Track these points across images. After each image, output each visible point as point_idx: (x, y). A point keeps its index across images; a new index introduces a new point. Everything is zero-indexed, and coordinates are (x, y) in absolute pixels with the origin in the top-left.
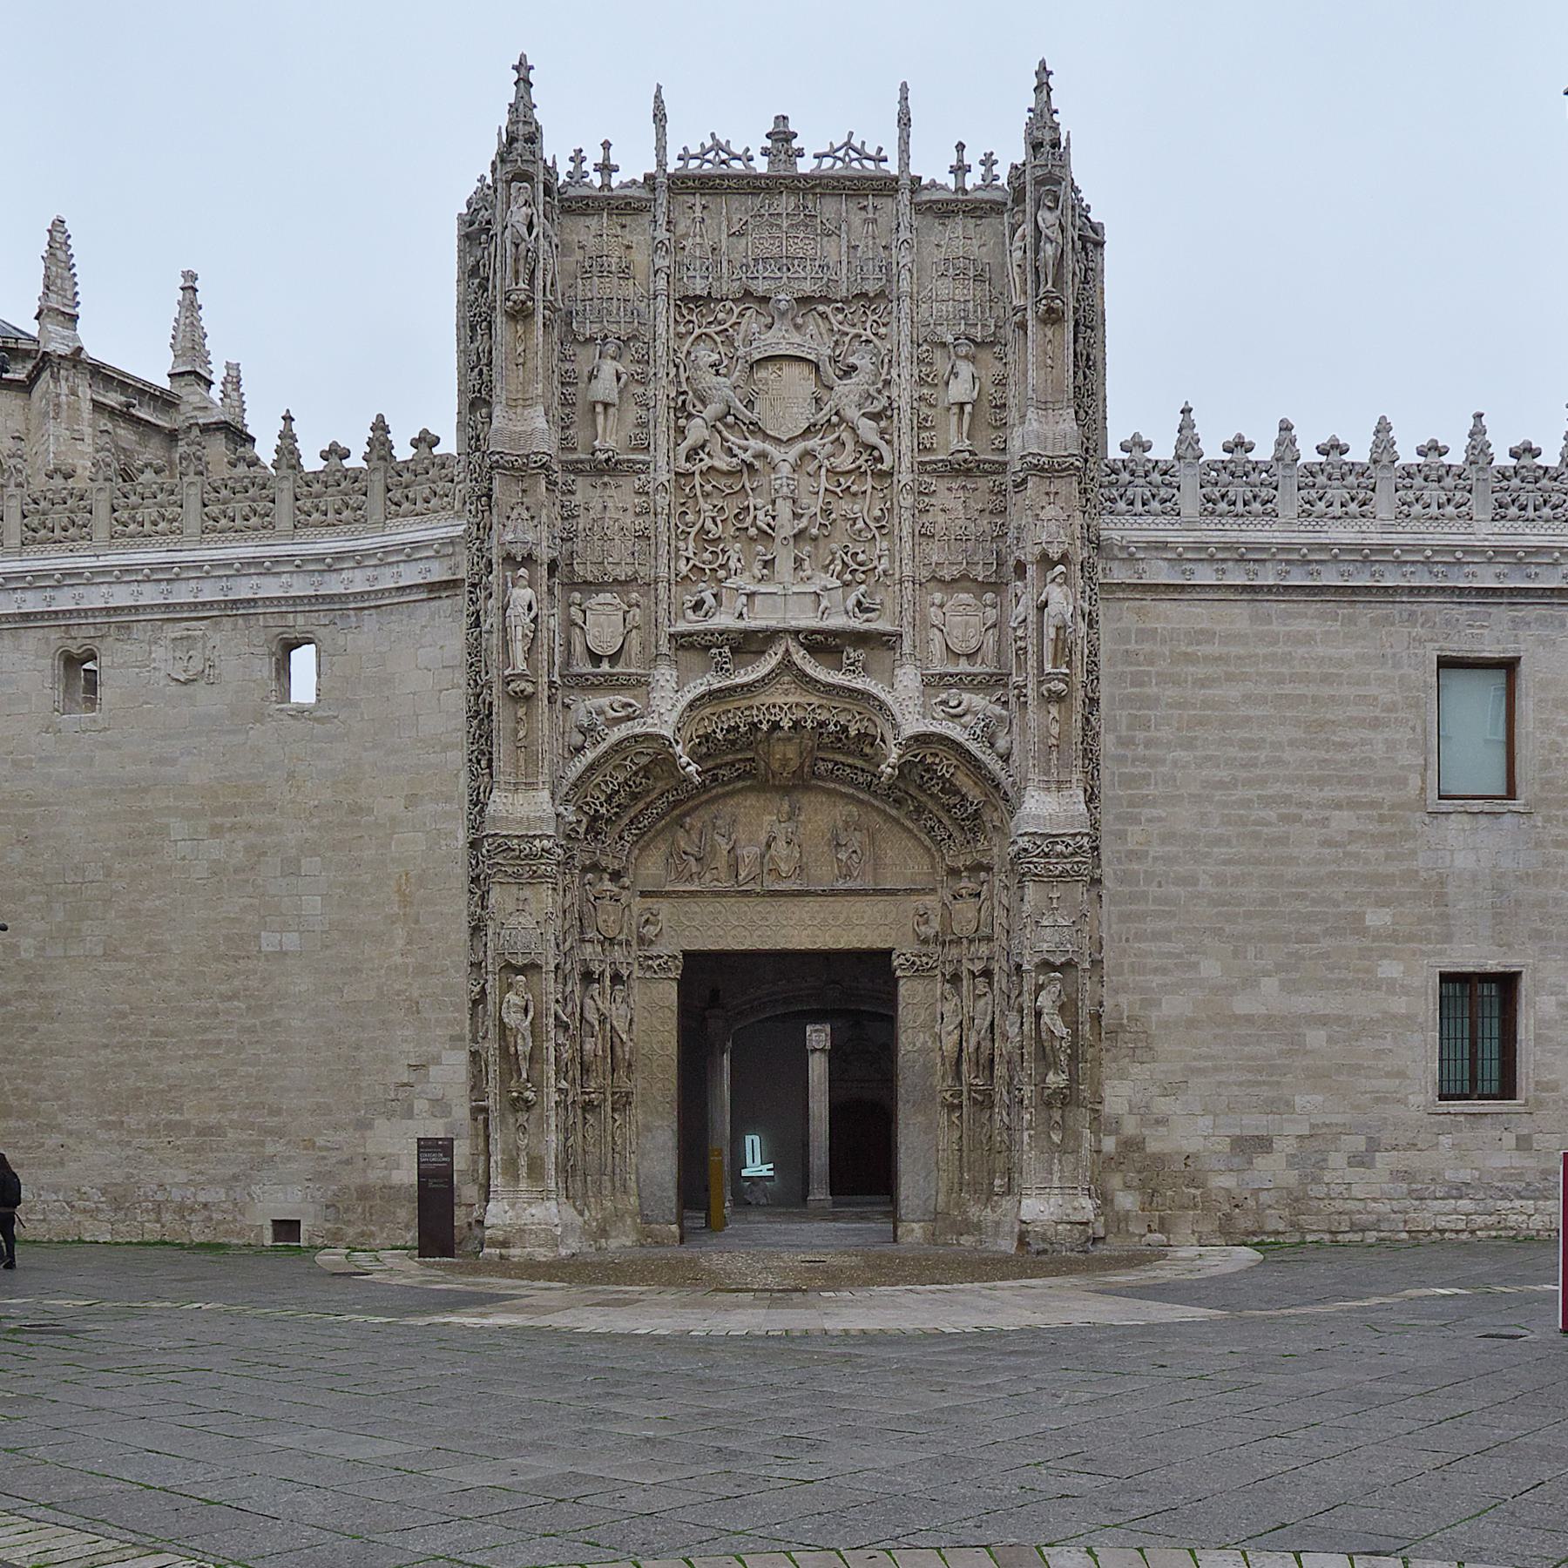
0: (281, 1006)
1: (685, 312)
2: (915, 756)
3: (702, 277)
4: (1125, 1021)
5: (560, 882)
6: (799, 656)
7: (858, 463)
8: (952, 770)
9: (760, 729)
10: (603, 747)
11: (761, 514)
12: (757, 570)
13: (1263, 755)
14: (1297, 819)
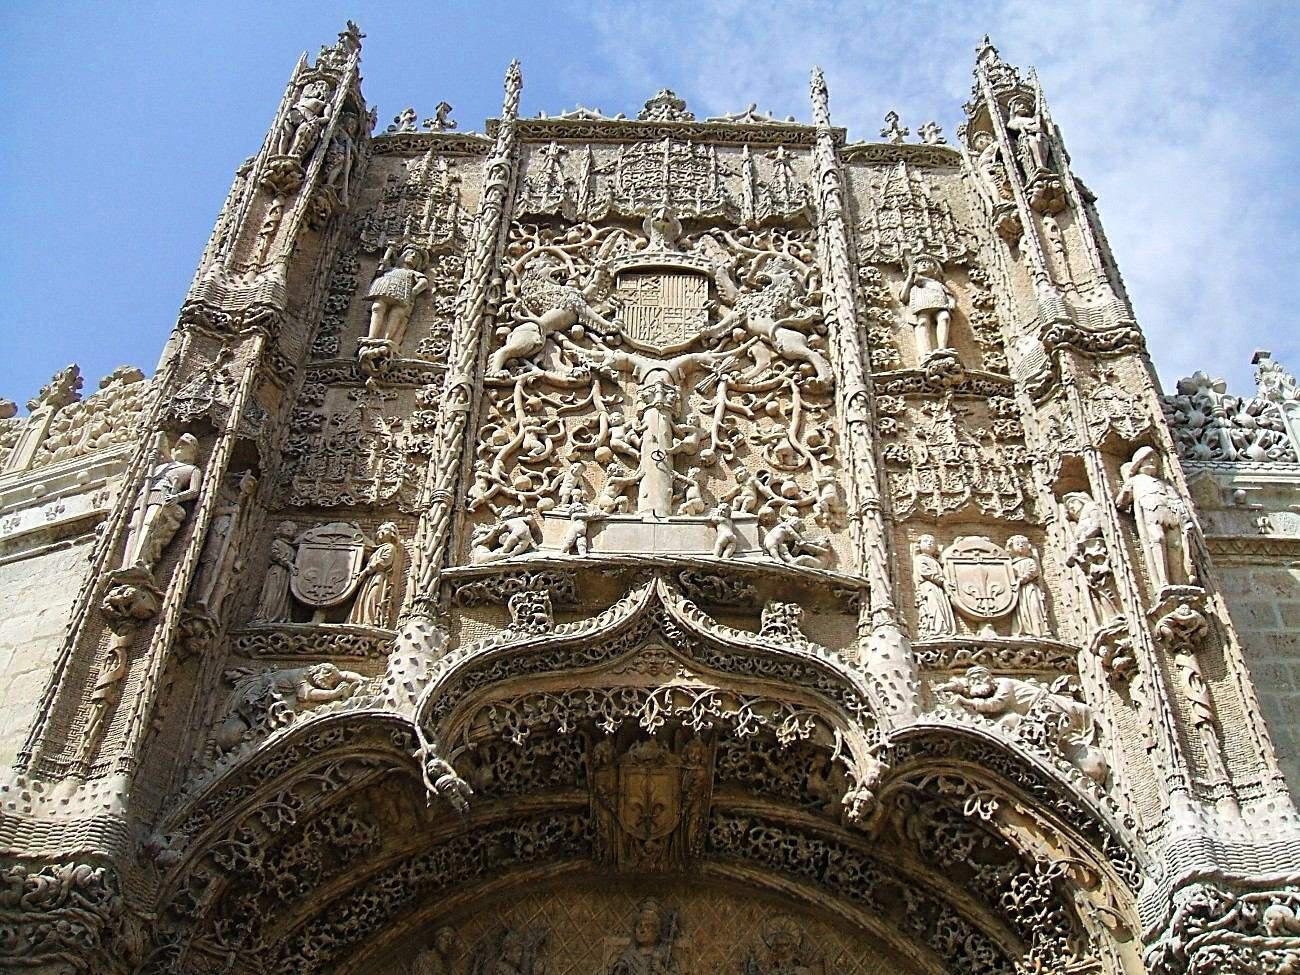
1: (521, 231)
2: (916, 780)
3: (552, 198)
6: (677, 607)
8: (993, 806)
9: (600, 735)
11: (617, 432)
12: (605, 497)
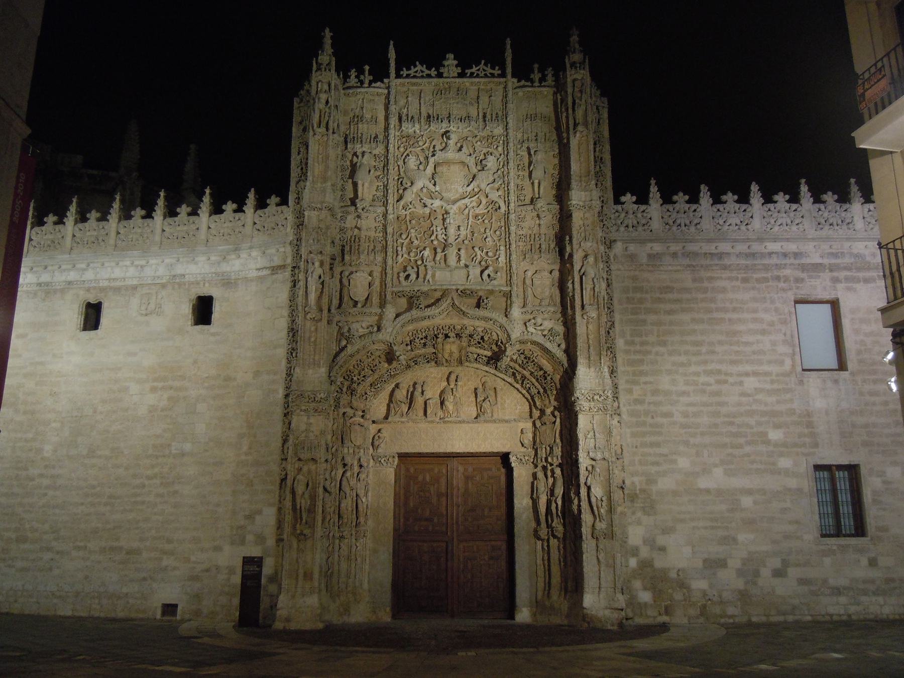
0: (179, 483)
4: (638, 492)
5: (331, 415)
7: (488, 209)
10: (356, 348)
13: (704, 349)
14: (726, 382)
